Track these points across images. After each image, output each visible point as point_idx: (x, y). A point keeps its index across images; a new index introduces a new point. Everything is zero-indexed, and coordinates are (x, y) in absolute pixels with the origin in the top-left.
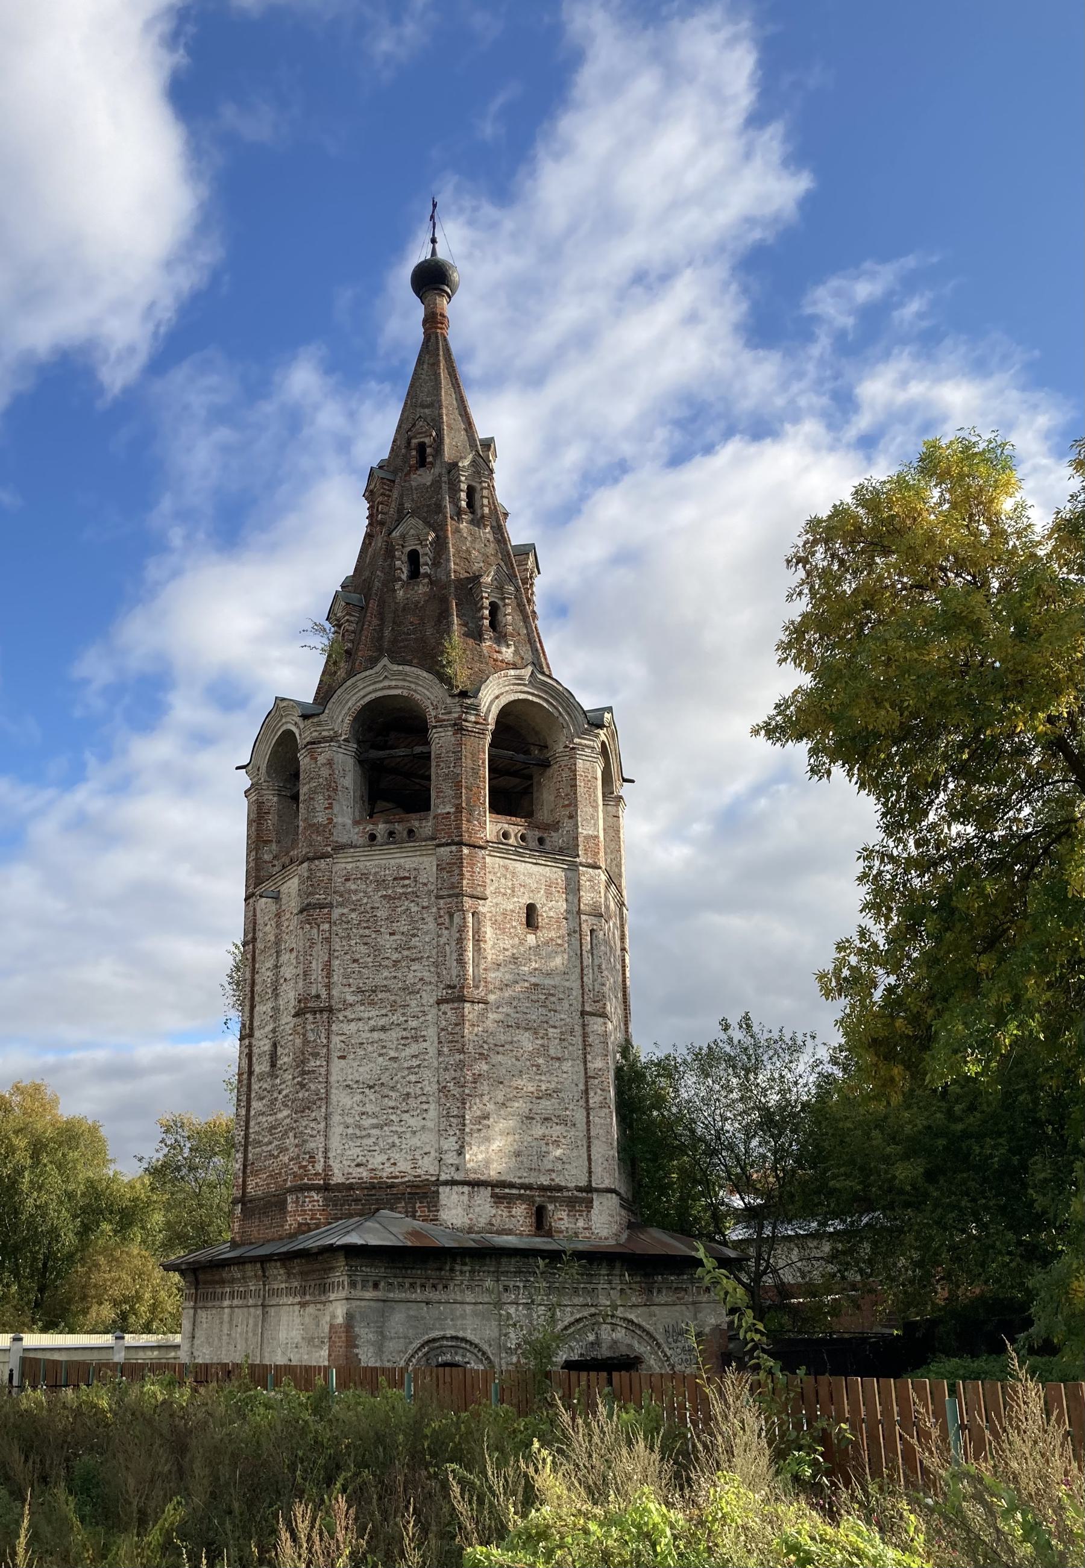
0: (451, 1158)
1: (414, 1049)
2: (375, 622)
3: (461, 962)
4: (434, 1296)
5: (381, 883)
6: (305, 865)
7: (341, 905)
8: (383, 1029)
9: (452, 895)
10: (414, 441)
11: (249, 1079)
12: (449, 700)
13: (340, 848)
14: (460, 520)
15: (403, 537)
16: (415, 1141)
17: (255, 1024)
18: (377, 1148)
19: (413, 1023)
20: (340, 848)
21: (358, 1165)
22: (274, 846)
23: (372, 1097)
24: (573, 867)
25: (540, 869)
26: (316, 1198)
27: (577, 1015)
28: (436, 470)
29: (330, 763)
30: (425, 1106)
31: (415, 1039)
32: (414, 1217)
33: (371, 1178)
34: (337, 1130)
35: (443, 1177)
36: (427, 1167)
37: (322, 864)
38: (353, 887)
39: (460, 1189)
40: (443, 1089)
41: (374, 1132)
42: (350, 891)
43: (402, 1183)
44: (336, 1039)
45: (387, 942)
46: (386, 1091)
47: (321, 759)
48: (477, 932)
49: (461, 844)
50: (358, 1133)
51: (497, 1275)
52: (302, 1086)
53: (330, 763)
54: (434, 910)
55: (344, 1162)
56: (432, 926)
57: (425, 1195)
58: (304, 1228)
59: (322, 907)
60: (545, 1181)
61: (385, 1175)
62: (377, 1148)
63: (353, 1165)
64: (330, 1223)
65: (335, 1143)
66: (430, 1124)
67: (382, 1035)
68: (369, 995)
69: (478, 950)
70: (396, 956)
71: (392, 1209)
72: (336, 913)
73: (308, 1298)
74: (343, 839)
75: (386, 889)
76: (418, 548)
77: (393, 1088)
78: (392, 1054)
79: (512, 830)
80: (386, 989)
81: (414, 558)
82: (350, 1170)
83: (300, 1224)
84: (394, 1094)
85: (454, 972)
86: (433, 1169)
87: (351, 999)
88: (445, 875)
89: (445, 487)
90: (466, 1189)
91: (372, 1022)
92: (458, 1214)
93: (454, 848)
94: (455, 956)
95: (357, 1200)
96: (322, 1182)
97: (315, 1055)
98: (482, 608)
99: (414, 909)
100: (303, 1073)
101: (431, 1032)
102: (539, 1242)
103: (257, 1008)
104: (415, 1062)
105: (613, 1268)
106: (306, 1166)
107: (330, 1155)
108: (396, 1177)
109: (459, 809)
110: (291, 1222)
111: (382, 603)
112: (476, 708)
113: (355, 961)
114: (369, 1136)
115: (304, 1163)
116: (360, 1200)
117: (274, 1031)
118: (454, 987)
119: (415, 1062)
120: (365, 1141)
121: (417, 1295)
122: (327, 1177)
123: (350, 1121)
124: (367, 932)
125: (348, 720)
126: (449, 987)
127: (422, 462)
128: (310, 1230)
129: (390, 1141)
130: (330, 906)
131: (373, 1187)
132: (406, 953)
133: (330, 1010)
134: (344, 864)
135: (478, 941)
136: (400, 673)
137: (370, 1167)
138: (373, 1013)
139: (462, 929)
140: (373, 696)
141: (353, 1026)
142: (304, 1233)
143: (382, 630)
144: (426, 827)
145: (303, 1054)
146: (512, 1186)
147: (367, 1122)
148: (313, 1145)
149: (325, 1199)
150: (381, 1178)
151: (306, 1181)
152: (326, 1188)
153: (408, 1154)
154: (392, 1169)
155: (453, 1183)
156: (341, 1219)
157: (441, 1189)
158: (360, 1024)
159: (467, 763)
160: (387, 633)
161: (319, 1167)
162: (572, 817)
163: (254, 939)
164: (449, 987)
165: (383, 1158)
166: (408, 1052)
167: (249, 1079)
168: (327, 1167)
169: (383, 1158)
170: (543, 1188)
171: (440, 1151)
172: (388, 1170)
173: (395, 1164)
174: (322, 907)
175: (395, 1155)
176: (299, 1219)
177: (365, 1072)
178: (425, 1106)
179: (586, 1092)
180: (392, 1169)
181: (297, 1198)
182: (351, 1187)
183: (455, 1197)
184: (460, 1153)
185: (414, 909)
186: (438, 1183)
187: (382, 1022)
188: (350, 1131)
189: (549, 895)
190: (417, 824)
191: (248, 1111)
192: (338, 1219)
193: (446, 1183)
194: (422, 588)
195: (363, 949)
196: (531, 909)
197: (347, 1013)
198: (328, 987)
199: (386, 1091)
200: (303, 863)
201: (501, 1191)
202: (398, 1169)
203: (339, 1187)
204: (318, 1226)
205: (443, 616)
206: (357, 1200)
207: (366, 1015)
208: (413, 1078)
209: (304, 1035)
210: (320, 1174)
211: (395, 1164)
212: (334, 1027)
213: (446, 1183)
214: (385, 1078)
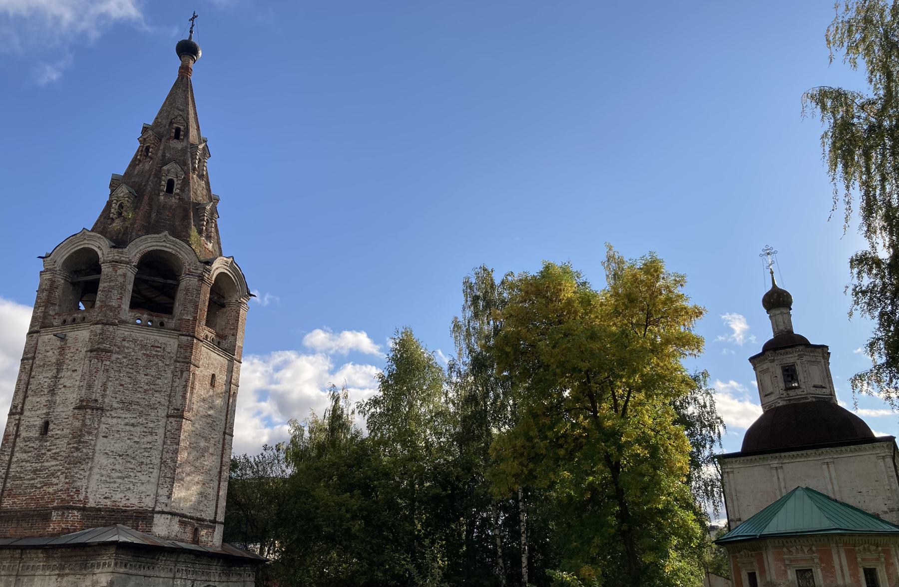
0: (163, 499)
1: (149, 438)
2: (147, 208)
3: (184, 397)
4: (149, 573)
5: (143, 347)
6: (100, 326)
7: (118, 353)
8: (133, 425)
9: (184, 362)
10: (175, 125)
11: (15, 439)
12: (198, 263)
13: (122, 322)
14: (194, 173)
15: (168, 171)
16: (142, 488)
17: (25, 407)
19: (151, 425)
20: (122, 322)
21: (105, 498)
22: (57, 308)
23: (121, 462)
24: (231, 361)
25: (218, 357)
27: (222, 433)
28: (185, 144)
29: (125, 275)
30: (151, 470)
31: (151, 433)
32: (137, 529)
34: (96, 477)
35: (157, 509)
36: (148, 503)
37: (111, 328)
38: (127, 345)
39: (166, 516)
40: (163, 462)
41: (119, 481)
42: (124, 347)
44: (103, 426)
45: (142, 378)
46: (129, 459)
47: (120, 272)
48: (193, 383)
49: (194, 337)
50: (108, 480)
51: (176, 562)
52: (77, 449)
53: (125, 275)
54: (172, 367)
56: (170, 375)
57: (145, 518)
58: (66, 531)
59: (107, 351)
60: (198, 515)
65: (93, 485)
66: (153, 480)
67: (132, 429)
68: (127, 405)
69: (192, 393)
70: (146, 387)
71: (124, 524)
72: (114, 356)
73: (67, 571)
74: (124, 318)
75: (146, 350)
76: (175, 180)
77: (133, 458)
78: (136, 439)
79: (210, 335)
80: (138, 404)
81: (170, 184)
83: (63, 529)
84: (134, 462)
85: (179, 402)
86: (151, 505)
87: (115, 405)
88: (182, 351)
89: (189, 154)
90: (169, 516)
91: (126, 421)
92: (163, 529)
93: (189, 338)
94: (181, 394)
95: (103, 518)
97: (89, 433)
98: (203, 220)
99: (161, 364)
100: (80, 442)
101: (161, 432)
102: (193, 547)
103: (30, 398)
104: (149, 446)
105: (219, 561)
109: (195, 319)
110: (52, 527)
111: (151, 199)
112: (209, 271)
113: (122, 385)
114: (115, 482)
117: (48, 414)
118: (178, 410)
119: (149, 446)
120: (112, 485)
121: (142, 572)
122: (85, 503)
123: (104, 473)
124: (131, 371)
125: (138, 256)
126: (175, 409)
127: (177, 136)
130: (111, 352)
131: (113, 510)
132: (152, 387)
133: (102, 409)
134: (122, 332)
135: (192, 388)
136: (173, 241)
138: (128, 416)
139: (187, 381)
140: (155, 248)
141: (115, 421)
143: (150, 213)
144: (172, 323)
145: (81, 431)
146: (186, 517)
147: (115, 475)
148: (79, 484)
152: (84, 509)
153: (136, 494)
155: (163, 512)
157: (155, 515)
158: (119, 420)
159: (202, 297)
160: (153, 215)
161: (81, 497)
162: (234, 335)
163: (34, 358)
164: (175, 409)
165: (122, 495)
166: (146, 439)
167: (15, 439)
168: (86, 497)
169: (122, 495)
170: (198, 520)
171: (157, 495)
172: (124, 502)
174: (107, 351)
175: (129, 494)
177: (118, 447)
178: (151, 470)
179: (220, 472)
182: (99, 510)
183: (162, 520)
184: (169, 497)
185: (161, 364)
186: (153, 511)
187: (133, 421)
188: (104, 478)
189: (221, 371)
190: (166, 320)
191: (11, 458)
192: (88, 527)
193: (159, 512)
194: (174, 201)
195: (128, 380)
196: (213, 376)
197: (114, 414)
198: (103, 396)
199: (129, 459)
200: (96, 324)
201: (184, 519)
203: (92, 509)
204: (75, 531)
205: (186, 217)
206: (103, 518)
207: (124, 416)
208: (146, 454)
209: (83, 421)
212: (103, 419)
213: (159, 512)
214: (130, 452)
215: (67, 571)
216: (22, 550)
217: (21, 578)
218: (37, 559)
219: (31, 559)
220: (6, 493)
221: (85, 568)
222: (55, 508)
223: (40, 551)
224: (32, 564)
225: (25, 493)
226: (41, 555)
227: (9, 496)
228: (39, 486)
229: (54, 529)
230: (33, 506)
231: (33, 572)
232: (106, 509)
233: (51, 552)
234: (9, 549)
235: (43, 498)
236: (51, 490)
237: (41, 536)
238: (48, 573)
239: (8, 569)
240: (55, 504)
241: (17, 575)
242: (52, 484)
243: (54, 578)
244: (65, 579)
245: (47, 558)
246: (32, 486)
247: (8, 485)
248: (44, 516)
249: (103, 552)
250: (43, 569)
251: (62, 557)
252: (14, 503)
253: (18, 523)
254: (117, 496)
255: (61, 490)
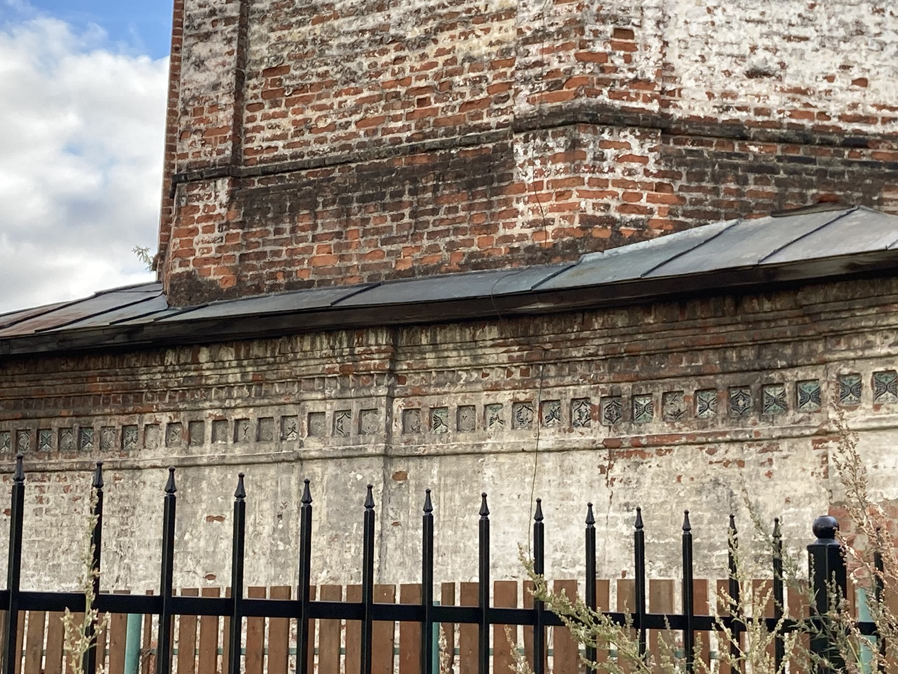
18: (809, 32)
21: (754, 74)
26: (636, 151)
33: (794, 113)
43: (885, 137)
55: (713, 61)
58: (605, 233)
61: (834, 109)
62: (809, 32)
63: (739, 70)
64: (682, 227)
73: (656, 427)
82: (732, 86)
83: (588, 222)
95: (763, 170)
96: (654, 107)
106: (605, 56)
107: (673, 34)
108: (868, 120)
115: (599, 48)
116: (773, 170)
122: (666, 98)
128: (618, 240)
129: (849, 18)
131: (803, 137)
137: (789, 82)
142: (601, 245)
149: (665, 157)
150: (823, 115)
151: (604, 97)
152: (660, 126)
154: (856, 96)
156: (716, 216)
165: (830, 61)
168: (666, 70)
169: (830, 61)
173: (863, 82)
175: (864, 58)
176: (587, 205)
180: (856, 96)
181: (575, 144)
182: (736, 132)
192: (705, 217)
202: (871, 98)
203: (699, 129)
204: (642, 232)
206: (763, 170)
210: (648, 83)
211: (863, 82)
215: (656, 427)
216: (394, 330)
217: (411, 468)
218: (480, 374)
219: (447, 375)
220: (254, 89)
221: (760, 409)
222: (524, 126)
223: (492, 333)
224: (452, 402)
225: (351, 78)
226: (495, 355)
227: (274, 97)
228: (413, 33)
229: (539, 225)
230: (401, 128)
231: (465, 440)
232: (768, 133)
233: (547, 333)
234: (331, 331)
235: (445, 89)
236: (480, 45)
237: (478, 264)
238: (548, 438)
239: (338, 429)
240: (522, 106)
241: (387, 457)
242: (480, 18)
243: (587, 464)
244: (654, 463)
245: (534, 365)
246: (380, 38)
247: (260, 50)
248: (480, 169)
249: (867, 318)
250: (518, 422)
251: (612, 358)
252: (303, 126)
253: (344, 214)
254: (810, 66)
255: (540, 36)
